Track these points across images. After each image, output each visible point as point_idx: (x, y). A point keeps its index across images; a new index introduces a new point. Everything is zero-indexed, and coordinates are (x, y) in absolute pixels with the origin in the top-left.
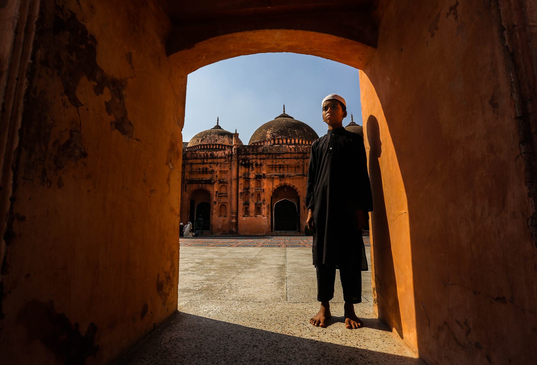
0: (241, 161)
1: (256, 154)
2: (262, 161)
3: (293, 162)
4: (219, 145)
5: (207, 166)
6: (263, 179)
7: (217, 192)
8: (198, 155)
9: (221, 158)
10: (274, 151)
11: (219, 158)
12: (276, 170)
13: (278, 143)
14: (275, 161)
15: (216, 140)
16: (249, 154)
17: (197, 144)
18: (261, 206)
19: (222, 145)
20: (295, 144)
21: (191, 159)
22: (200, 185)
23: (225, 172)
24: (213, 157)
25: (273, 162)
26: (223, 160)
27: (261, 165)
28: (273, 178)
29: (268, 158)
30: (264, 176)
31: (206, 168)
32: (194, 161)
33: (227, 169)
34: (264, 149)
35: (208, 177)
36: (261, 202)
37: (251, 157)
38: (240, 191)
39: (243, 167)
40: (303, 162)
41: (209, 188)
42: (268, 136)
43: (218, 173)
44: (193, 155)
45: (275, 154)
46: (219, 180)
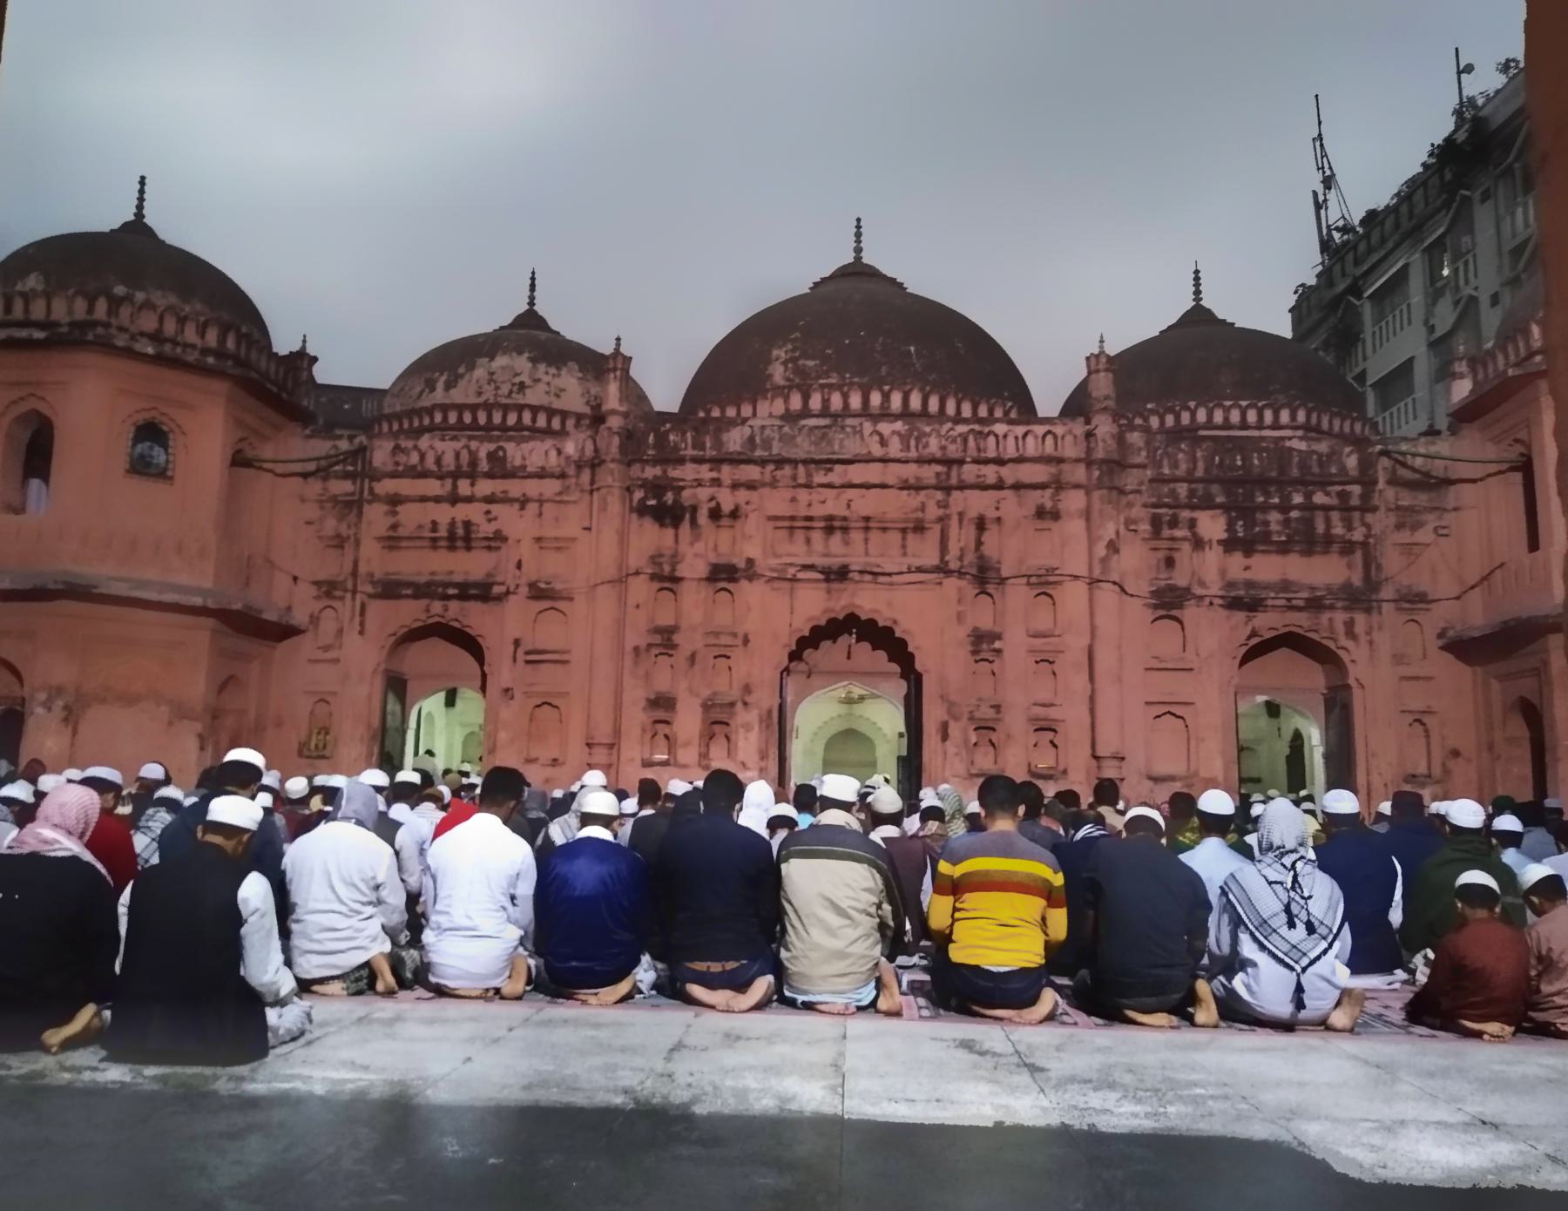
1: (716, 462)
2: (743, 495)
3: (896, 505)
4: (535, 410)
5: (474, 512)
6: (744, 583)
9: (542, 474)
10: (804, 447)
12: (808, 541)
13: (825, 412)
14: (803, 495)
15: (522, 386)
16: (681, 461)
17: (426, 402)
18: (732, 715)
19: (551, 412)
20: (905, 414)
21: (394, 475)
22: (437, 606)
23: (561, 545)
24: (500, 468)
25: (793, 500)
26: (550, 487)
27: (735, 514)
28: (794, 580)
29: (773, 484)
30: (749, 571)
31: (467, 525)
32: (405, 486)
33: (571, 528)
34: (751, 439)
35: (471, 565)
36: (735, 694)
37: (687, 472)
39: (649, 525)
40: (943, 505)
41: (474, 617)
42: (778, 373)
43: (526, 551)
44: (402, 458)
45: (805, 462)
46: (532, 585)
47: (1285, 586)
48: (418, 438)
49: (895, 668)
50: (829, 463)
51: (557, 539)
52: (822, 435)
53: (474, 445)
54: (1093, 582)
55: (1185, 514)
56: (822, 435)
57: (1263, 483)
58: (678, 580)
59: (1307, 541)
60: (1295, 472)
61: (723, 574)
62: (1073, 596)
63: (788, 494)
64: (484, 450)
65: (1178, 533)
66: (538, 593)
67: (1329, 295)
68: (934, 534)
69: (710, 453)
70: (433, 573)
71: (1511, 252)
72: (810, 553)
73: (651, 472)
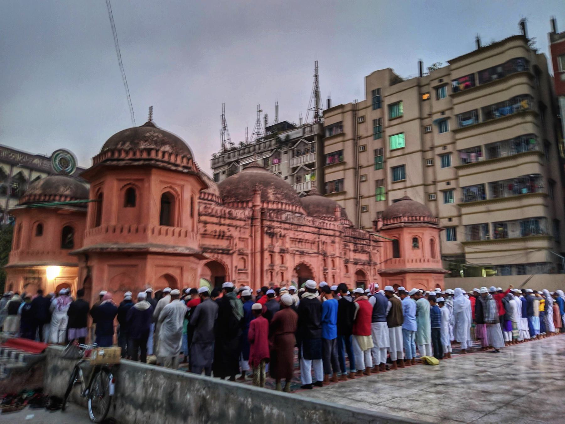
0: (266, 229)
2: (286, 232)
7: (236, 267)
8: (214, 211)
9: (240, 220)
10: (295, 221)
11: (237, 220)
14: (297, 233)
16: (274, 221)
21: (205, 215)
22: (216, 256)
24: (231, 218)
26: (242, 223)
27: (284, 236)
28: (295, 254)
29: (291, 229)
31: (224, 232)
36: (284, 283)
37: (275, 224)
38: (266, 267)
40: (319, 238)
42: (271, 197)
43: (237, 241)
47: (360, 260)
48: (211, 204)
49: (296, 275)
50: (300, 226)
51: (244, 238)
52: (299, 219)
53: (225, 209)
54: (340, 257)
55: (349, 244)
56: (299, 219)
57: (358, 238)
58: (273, 252)
59: (363, 251)
60: (361, 237)
61: (283, 251)
62: (337, 261)
63: (293, 232)
64: (228, 210)
65: (347, 248)
66: (241, 253)
67: (228, 161)
68: (316, 244)
69: (279, 220)
70: (214, 245)
71: (292, 168)
72: (296, 247)
73: (268, 223)
